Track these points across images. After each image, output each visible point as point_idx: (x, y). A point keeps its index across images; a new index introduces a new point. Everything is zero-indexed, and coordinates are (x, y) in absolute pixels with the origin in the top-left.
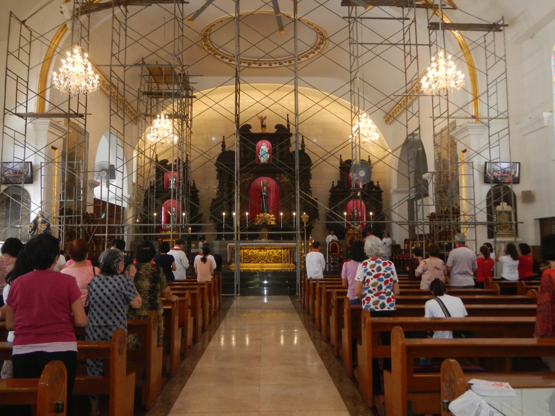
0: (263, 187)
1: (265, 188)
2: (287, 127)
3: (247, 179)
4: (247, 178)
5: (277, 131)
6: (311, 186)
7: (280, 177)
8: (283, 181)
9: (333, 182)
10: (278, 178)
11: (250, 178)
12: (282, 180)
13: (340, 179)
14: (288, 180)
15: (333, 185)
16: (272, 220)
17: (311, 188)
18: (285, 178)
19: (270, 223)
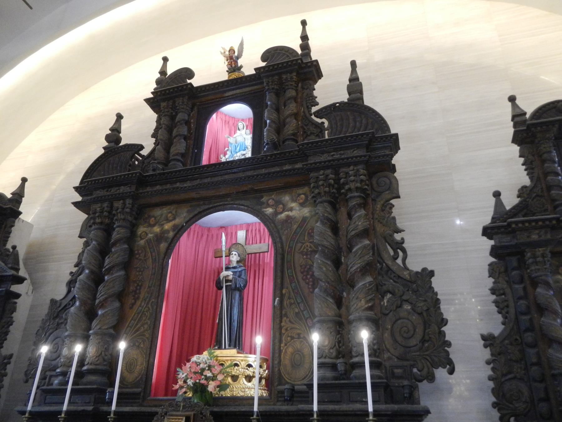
0: (229, 255)
1: (235, 258)
2: (299, 52)
3: (167, 227)
4: (168, 221)
5: (266, 64)
6: (400, 224)
7: (278, 203)
8: (288, 217)
9: (497, 194)
10: (269, 211)
11: (177, 221)
12: (283, 216)
13: (526, 181)
14: (306, 211)
15: (499, 204)
16: (249, 378)
17: (399, 231)
18: (293, 205)
19: (223, 387)
